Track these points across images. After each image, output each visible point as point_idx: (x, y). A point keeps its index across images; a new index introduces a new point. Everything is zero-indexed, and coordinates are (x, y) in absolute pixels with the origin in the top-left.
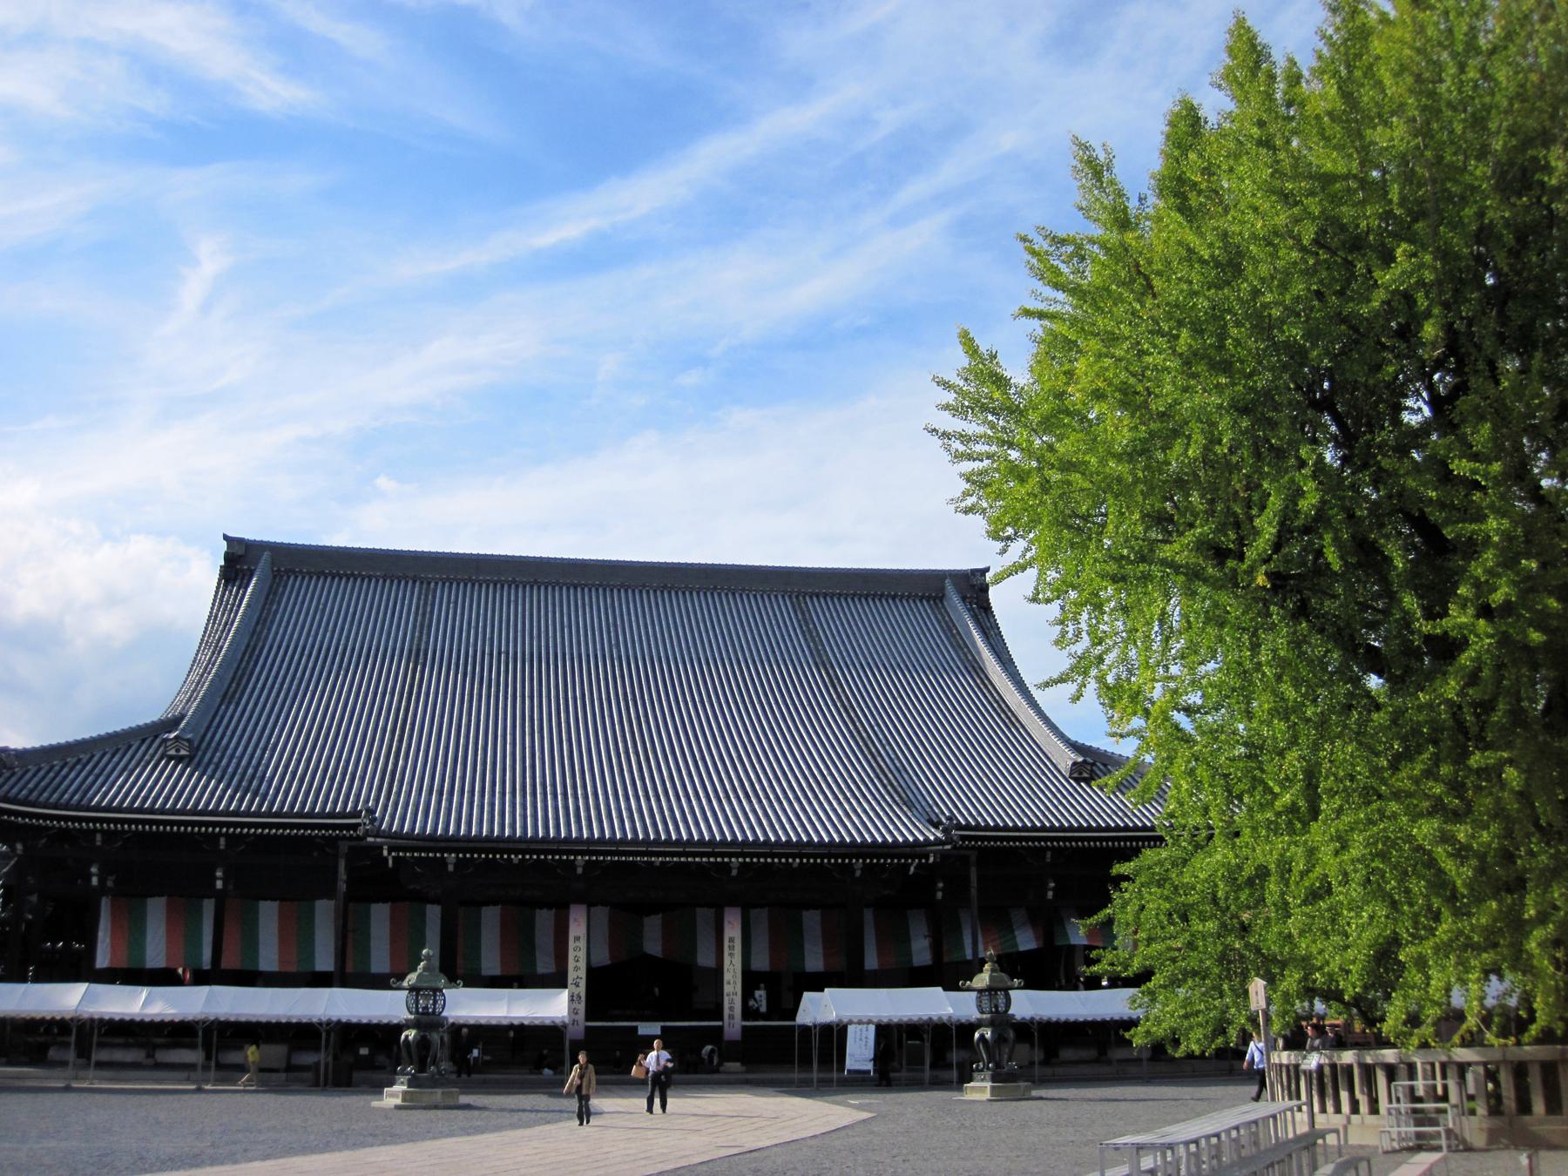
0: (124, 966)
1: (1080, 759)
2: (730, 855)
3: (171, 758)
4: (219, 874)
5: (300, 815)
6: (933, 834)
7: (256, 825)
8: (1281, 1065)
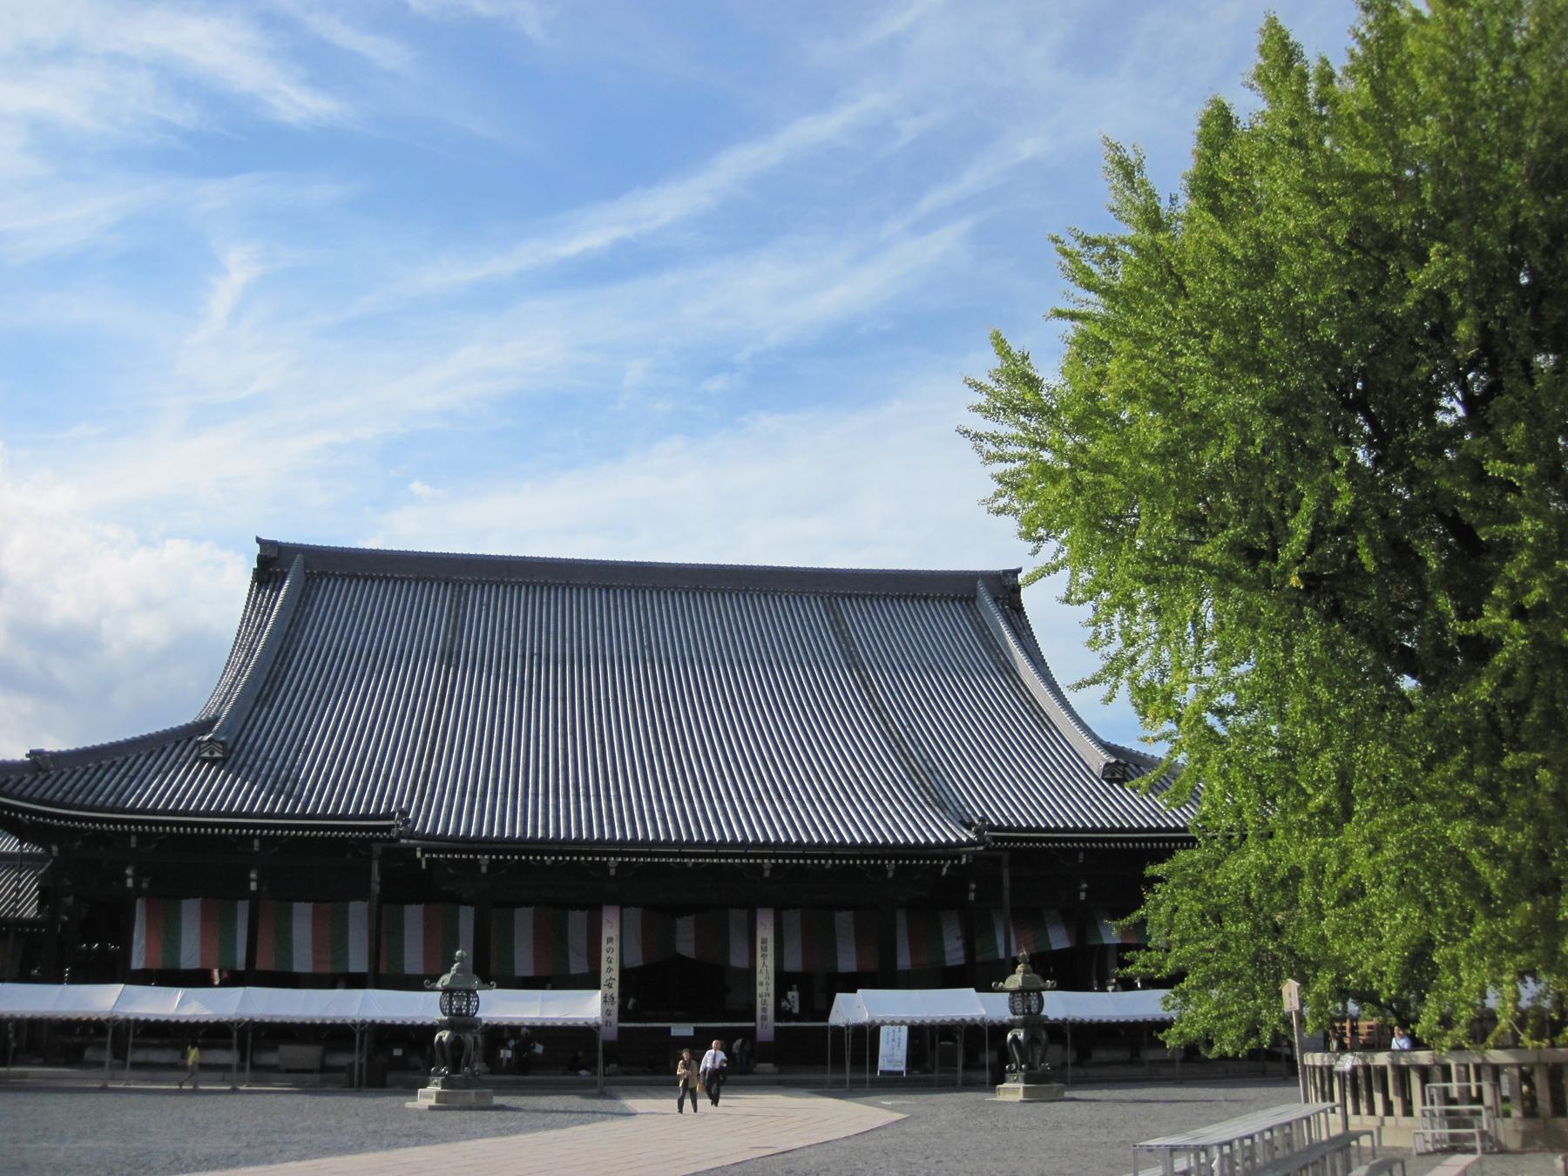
0: (160, 967)
1: (1113, 760)
2: (763, 856)
3: (205, 760)
4: (253, 875)
5: (334, 817)
6: (966, 835)
7: (290, 827)
8: (1314, 1067)
